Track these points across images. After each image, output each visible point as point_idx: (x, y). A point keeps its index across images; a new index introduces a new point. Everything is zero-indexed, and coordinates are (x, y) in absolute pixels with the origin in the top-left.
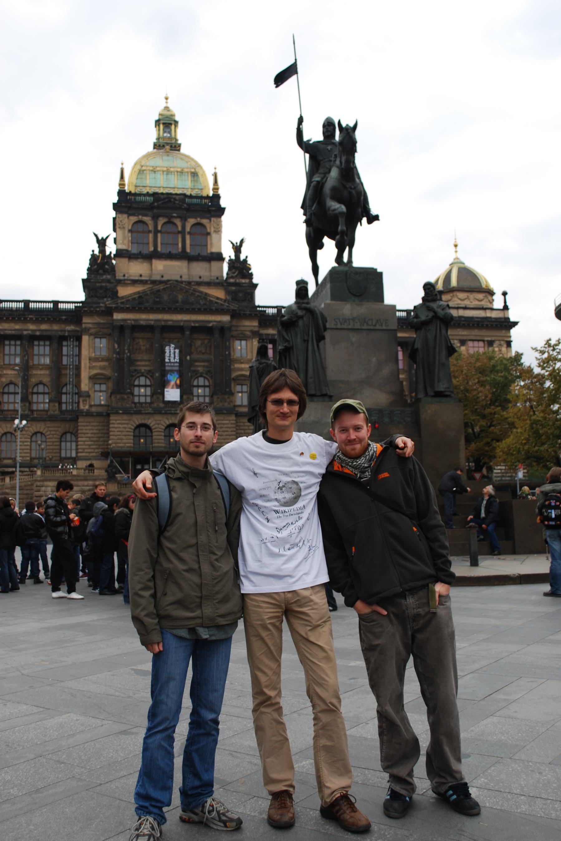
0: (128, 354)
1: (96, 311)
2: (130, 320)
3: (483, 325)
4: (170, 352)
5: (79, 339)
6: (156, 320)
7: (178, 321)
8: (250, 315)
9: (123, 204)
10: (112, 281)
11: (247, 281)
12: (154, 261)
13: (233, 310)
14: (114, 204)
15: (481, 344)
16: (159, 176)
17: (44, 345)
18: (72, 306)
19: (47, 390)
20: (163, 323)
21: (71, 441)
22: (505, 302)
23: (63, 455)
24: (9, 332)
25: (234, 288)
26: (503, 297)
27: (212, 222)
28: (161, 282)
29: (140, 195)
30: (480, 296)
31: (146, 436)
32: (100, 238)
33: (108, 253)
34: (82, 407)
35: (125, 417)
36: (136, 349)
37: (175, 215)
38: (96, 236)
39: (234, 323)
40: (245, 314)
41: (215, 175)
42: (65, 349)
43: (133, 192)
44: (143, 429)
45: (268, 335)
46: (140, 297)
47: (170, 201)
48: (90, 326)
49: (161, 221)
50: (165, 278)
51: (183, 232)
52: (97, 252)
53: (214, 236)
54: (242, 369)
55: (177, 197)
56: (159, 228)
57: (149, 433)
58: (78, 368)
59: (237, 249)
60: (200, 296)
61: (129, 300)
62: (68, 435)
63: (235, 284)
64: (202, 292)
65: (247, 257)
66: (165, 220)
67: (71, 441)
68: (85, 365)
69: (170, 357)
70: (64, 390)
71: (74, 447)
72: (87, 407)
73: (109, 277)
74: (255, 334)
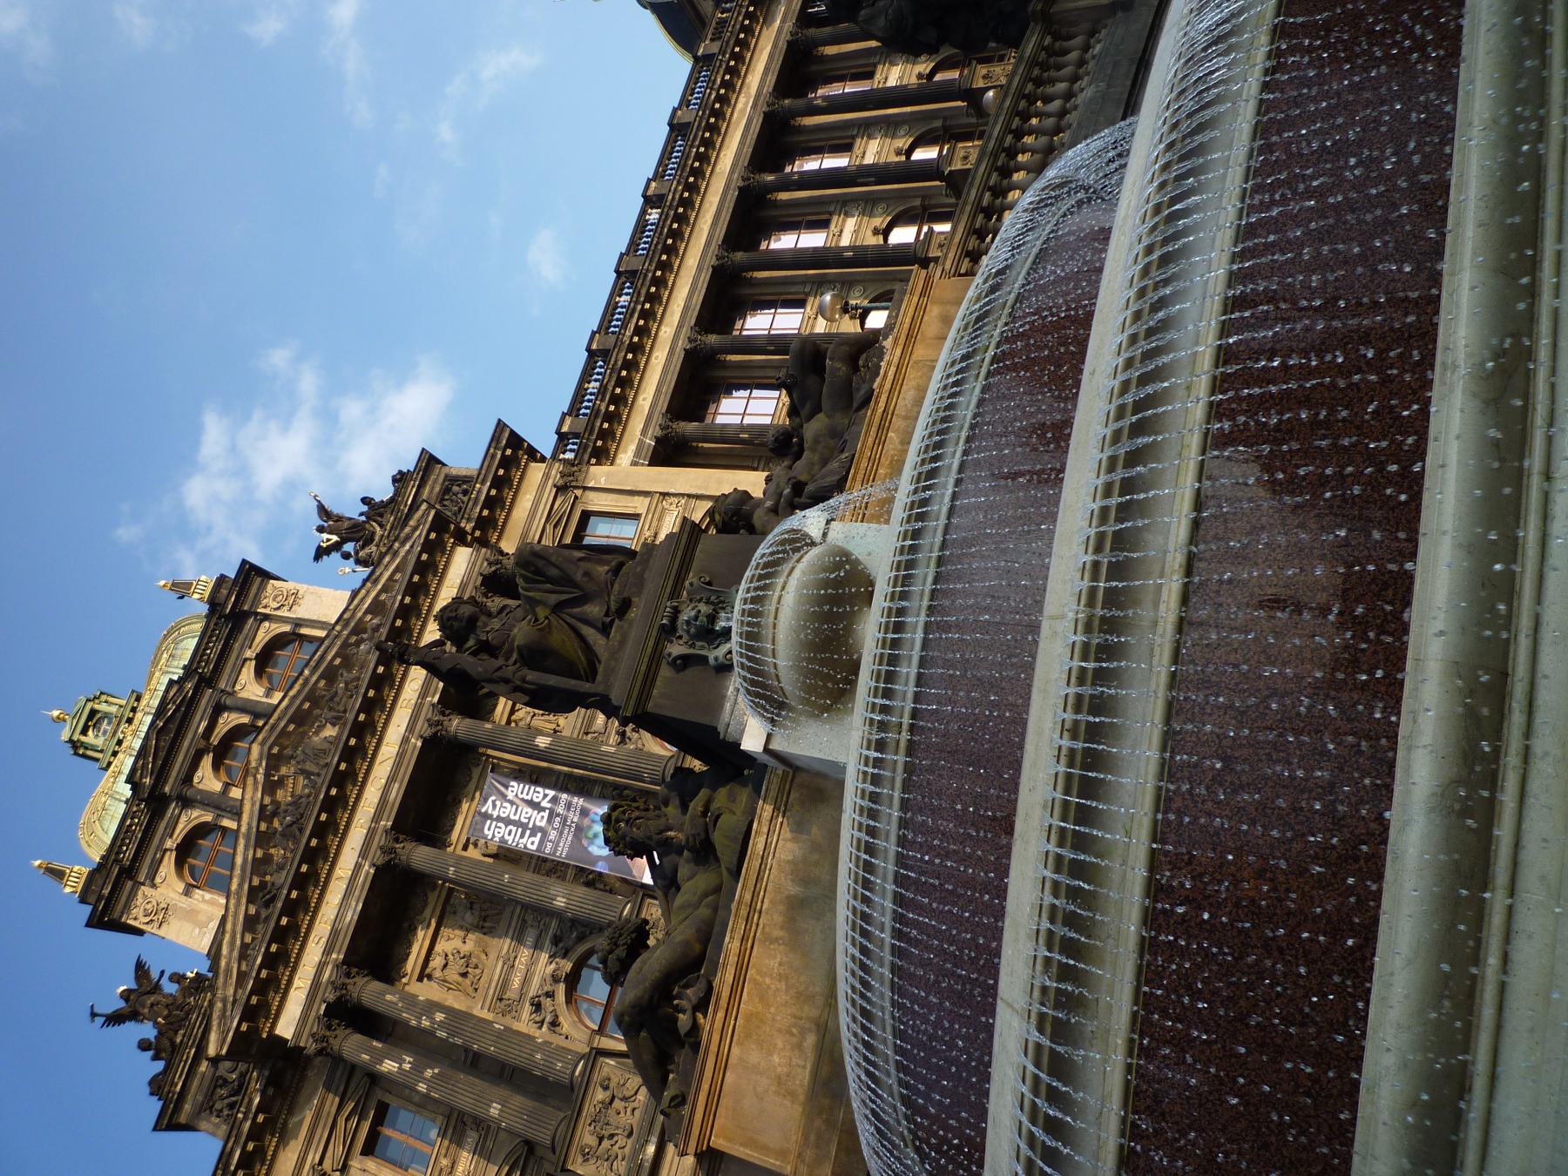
0: (439, 1017)
1: (259, 1110)
2: (321, 967)
4: (507, 821)
6: (363, 854)
7: (401, 755)
8: (498, 483)
9: (106, 892)
14: (88, 925)
20: (386, 823)
27: (267, 611)
32: (122, 1004)
36: (464, 975)
37: (201, 730)
38: (115, 1019)
40: (490, 503)
47: (161, 732)
48: (313, 1157)
49: (207, 779)
53: (300, 612)
60: (345, 645)
61: (244, 946)
65: (365, 500)
66: (207, 761)
69: (524, 826)
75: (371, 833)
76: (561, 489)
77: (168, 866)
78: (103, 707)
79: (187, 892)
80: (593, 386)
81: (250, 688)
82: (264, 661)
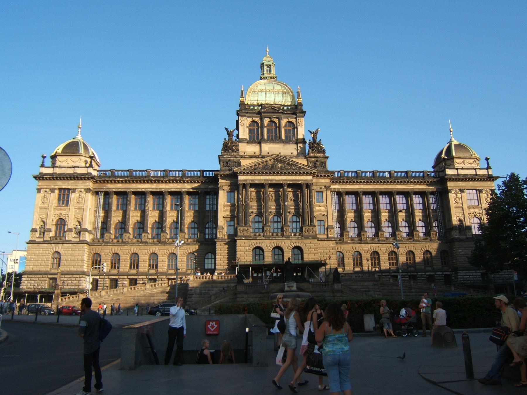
3: (475, 179)
5: (217, 194)
7: (279, 180)
8: (325, 176)
10: (237, 156)
11: (322, 155)
12: (262, 144)
13: (314, 173)
15: (474, 191)
16: (264, 94)
17: (195, 198)
18: (212, 174)
19: (196, 226)
21: (211, 259)
22: (488, 164)
23: (206, 267)
24: (173, 190)
25: (313, 159)
26: (486, 161)
28: (267, 156)
29: (253, 105)
30: (471, 161)
31: (259, 255)
33: (234, 140)
34: (218, 236)
35: (246, 241)
39: (315, 180)
40: (321, 176)
41: (298, 92)
42: (208, 201)
43: (249, 104)
44: (257, 250)
45: (335, 189)
46: (255, 165)
48: (224, 184)
50: (270, 154)
51: (280, 127)
52: (227, 139)
53: (299, 127)
54: (320, 211)
55: (276, 106)
56: (265, 125)
57: (261, 252)
58: (216, 212)
59: (315, 134)
60: (293, 164)
62: (210, 254)
63: (315, 157)
64: (294, 162)
65: (320, 140)
66: (269, 120)
67: (211, 259)
68: (221, 209)
70: (207, 226)
71: (213, 262)
72: (221, 236)
73: (235, 154)
74: (327, 188)
75: (267, 180)
76: (325, 186)
77: (250, 120)
78: (272, 67)
79: (247, 127)
80: (350, 175)
81: (284, 122)
82: (289, 122)
